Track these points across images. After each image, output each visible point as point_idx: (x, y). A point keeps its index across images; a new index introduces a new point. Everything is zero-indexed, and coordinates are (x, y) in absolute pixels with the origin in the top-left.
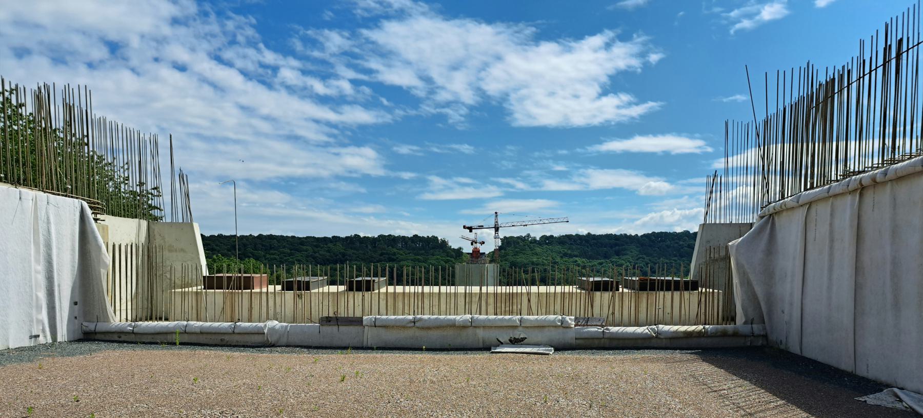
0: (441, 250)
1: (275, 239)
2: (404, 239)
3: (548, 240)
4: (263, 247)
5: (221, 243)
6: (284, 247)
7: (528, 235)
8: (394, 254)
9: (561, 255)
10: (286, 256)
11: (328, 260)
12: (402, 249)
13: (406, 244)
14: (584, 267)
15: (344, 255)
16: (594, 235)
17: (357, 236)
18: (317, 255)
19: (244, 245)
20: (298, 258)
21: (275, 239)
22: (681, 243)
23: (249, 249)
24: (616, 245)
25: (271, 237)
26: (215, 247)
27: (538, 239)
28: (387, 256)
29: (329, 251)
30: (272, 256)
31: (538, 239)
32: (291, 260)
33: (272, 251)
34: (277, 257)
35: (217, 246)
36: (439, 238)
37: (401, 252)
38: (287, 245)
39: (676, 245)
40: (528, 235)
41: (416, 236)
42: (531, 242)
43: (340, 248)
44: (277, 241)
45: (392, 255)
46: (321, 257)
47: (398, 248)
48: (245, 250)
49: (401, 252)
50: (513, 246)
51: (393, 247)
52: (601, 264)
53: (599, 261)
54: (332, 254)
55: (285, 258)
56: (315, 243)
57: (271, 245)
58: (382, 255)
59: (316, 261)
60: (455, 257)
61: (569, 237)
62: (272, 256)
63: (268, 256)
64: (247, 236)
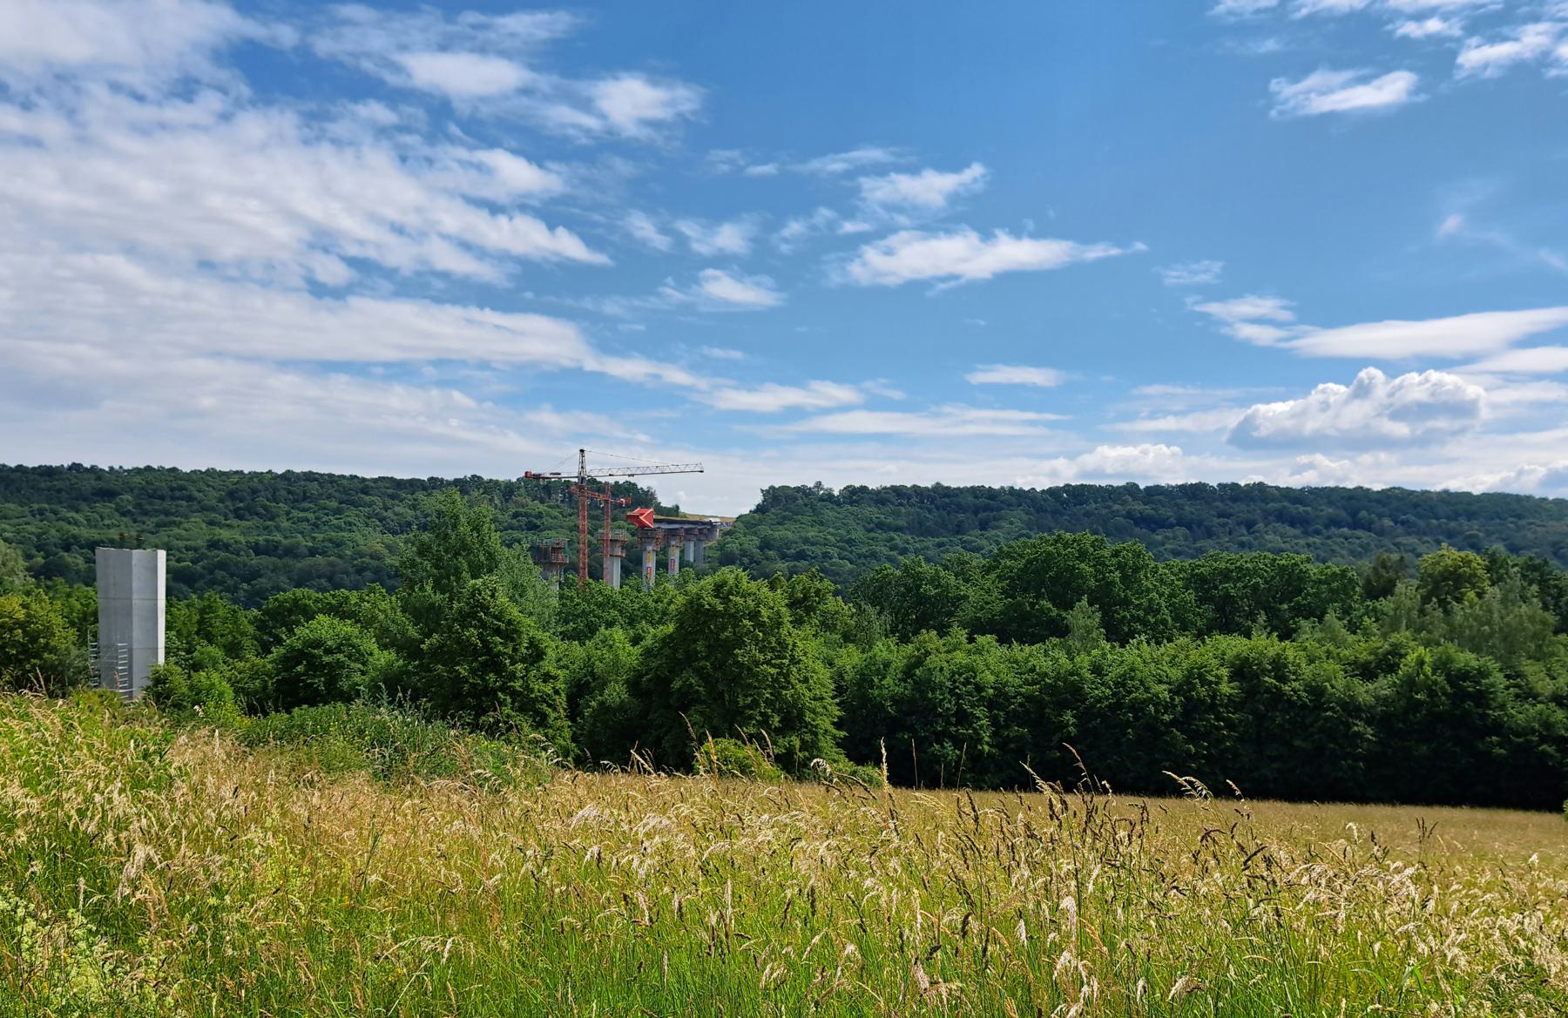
1: (316, 480)
3: (855, 495)
4: (290, 497)
5: (209, 486)
6: (329, 497)
8: (540, 515)
10: (327, 515)
12: (558, 507)
16: (948, 488)
17: (476, 480)
18: (389, 514)
19: (252, 490)
20: (349, 519)
21: (316, 480)
22: (1116, 507)
23: (262, 500)
24: (987, 508)
25: (310, 477)
26: (196, 494)
27: (836, 493)
29: (414, 507)
30: (302, 515)
31: (836, 493)
32: (335, 522)
33: (305, 505)
34: (311, 516)
35: (199, 491)
37: (555, 513)
38: (336, 494)
39: (1104, 511)
40: (819, 485)
42: (821, 499)
44: (320, 484)
46: (395, 518)
48: (253, 500)
49: (555, 513)
51: (542, 502)
53: (936, 540)
54: (418, 512)
55: (325, 519)
56: (390, 491)
57: (304, 492)
58: (516, 515)
59: (384, 525)
61: (898, 491)
62: (302, 515)
63: (295, 513)
64: (262, 473)
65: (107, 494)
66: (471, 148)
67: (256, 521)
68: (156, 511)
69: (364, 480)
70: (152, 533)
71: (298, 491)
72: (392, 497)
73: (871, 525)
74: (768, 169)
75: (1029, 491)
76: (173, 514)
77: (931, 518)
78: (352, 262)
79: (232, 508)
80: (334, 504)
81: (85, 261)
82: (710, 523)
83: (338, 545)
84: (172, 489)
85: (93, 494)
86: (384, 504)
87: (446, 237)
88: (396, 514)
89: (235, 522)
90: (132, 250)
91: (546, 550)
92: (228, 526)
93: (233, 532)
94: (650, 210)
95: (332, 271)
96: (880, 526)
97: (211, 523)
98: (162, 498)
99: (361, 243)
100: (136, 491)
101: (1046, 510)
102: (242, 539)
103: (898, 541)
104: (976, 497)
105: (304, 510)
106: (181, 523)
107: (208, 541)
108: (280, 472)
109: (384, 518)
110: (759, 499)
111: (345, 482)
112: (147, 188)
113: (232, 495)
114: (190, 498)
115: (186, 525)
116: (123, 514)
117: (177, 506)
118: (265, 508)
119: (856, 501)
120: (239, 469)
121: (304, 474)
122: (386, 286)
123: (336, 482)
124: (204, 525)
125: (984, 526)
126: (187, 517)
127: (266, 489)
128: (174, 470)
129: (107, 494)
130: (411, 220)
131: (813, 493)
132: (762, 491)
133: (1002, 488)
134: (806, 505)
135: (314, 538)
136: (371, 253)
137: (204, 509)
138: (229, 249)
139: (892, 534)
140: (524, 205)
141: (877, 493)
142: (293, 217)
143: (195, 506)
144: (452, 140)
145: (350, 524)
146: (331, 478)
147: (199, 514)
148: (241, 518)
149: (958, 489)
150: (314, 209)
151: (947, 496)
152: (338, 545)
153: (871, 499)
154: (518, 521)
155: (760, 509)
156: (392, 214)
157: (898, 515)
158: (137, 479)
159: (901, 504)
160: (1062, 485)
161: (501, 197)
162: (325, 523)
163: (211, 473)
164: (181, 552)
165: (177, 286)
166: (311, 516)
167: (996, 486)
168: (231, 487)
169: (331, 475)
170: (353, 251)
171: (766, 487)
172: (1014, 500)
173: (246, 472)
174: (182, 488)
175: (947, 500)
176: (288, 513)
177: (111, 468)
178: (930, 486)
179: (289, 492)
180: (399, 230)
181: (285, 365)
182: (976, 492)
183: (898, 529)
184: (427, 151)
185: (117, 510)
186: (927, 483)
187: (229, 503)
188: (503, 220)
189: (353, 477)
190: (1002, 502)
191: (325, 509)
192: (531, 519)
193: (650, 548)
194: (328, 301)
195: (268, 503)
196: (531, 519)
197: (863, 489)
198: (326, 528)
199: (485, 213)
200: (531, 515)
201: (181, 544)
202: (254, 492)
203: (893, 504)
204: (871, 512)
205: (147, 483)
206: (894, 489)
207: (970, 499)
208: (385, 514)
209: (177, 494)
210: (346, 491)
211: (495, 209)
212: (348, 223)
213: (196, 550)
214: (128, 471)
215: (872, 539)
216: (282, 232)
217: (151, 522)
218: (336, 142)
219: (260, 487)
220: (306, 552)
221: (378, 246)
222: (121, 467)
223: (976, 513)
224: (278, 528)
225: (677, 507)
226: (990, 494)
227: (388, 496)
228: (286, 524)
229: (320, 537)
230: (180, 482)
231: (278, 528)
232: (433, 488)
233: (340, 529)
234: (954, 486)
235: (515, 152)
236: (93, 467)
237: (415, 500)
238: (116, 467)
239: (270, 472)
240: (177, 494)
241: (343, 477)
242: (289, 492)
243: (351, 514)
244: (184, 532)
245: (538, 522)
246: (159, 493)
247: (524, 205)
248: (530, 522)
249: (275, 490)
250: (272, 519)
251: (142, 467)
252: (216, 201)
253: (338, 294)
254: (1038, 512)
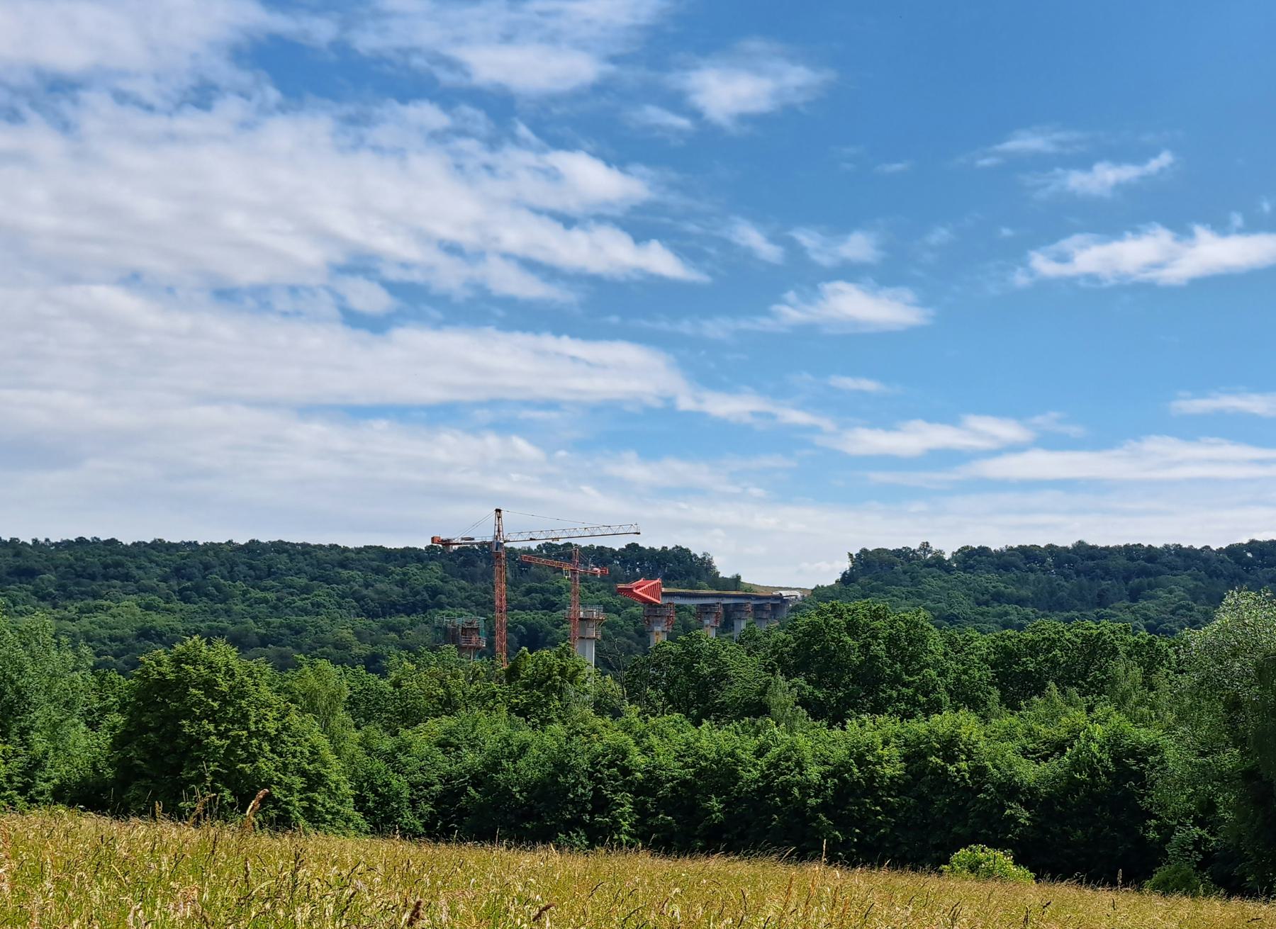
2: (601, 554)
3: (972, 558)
5: (151, 561)
6: (299, 572)
7: (925, 547)
10: (292, 594)
11: (393, 605)
15: (434, 592)
18: (368, 592)
20: (318, 599)
21: (286, 551)
23: (215, 577)
25: (280, 547)
26: (134, 572)
27: (947, 556)
29: (401, 584)
30: (261, 595)
31: (947, 556)
32: (299, 603)
33: (269, 582)
34: (271, 596)
35: (138, 568)
42: (927, 565)
43: (434, 573)
44: (290, 555)
45: (554, 594)
46: (376, 597)
48: (204, 578)
54: (407, 590)
56: (375, 564)
57: (270, 567)
58: (529, 592)
59: (362, 606)
61: (1028, 554)
62: (261, 595)
64: (220, 544)
65: (27, 574)
66: (541, 151)
67: (204, 603)
68: (82, 593)
69: (346, 549)
70: (73, 620)
71: (262, 566)
72: (377, 571)
73: (986, 597)
74: (897, 167)
75: (1201, 550)
76: (102, 597)
78: (393, 288)
79: (176, 588)
80: (303, 581)
81: (77, 295)
82: (780, 597)
83: (298, 633)
84: (106, 567)
85: (9, 574)
86: (365, 580)
87: (507, 256)
88: (378, 592)
89: (177, 605)
90: (132, 280)
91: (455, 630)
92: (167, 610)
93: (171, 617)
94: (758, 219)
95: (367, 297)
96: (998, 597)
97: (148, 607)
98: (93, 577)
99: (405, 265)
100: (62, 569)
101: (1222, 574)
102: (179, 626)
103: (1014, 618)
104: (1131, 559)
105: (264, 589)
106: (109, 608)
107: (138, 629)
108: (242, 543)
109: (363, 598)
110: (846, 565)
111: (320, 554)
112: (151, 208)
113: (179, 572)
114: (127, 577)
115: (114, 611)
116: (43, 598)
117: (109, 587)
118: (217, 587)
119: (972, 567)
120: (193, 540)
121: (273, 544)
122: (437, 314)
123: (308, 553)
124: (138, 610)
125: (1135, 596)
126: (119, 601)
127: (223, 564)
128: (113, 542)
129: (27, 574)
130: (467, 237)
131: (919, 557)
132: (851, 556)
133: (1166, 547)
134: (905, 572)
135: (268, 624)
136: (416, 276)
137: (143, 590)
138: (248, 273)
139: (1008, 608)
140: (599, 216)
141: (1000, 554)
142: (323, 236)
143: (131, 586)
144: (516, 141)
145: (319, 605)
146: (306, 550)
147: (135, 597)
148: (186, 600)
149: (1107, 548)
150: (350, 228)
151: (1092, 558)
152: (298, 633)
153: (992, 564)
154: (531, 599)
155: (846, 579)
156: (445, 231)
157: (1022, 582)
158: (65, 554)
159: (1032, 570)
160: (1245, 541)
161: (571, 204)
162: (287, 605)
163: (158, 545)
164: (105, 644)
165: (184, 322)
166: (271, 596)
167: (1158, 544)
168: (179, 561)
169: (305, 545)
170: (393, 274)
171: (855, 551)
172: (1179, 562)
173: (201, 543)
174: (118, 565)
175: (1091, 563)
176: (245, 593)
177: (35, 541)
178: (1070, 546)
179: (251, 567)
180: (452, 249)
181: (308, 410)
182: (1130, 552)
183: (1021, 602)
184: (486, 157)
185: (35, 593)
187: (173, 583)
188: (577, 235)
189: (334, 547)
190: (1164, 564)
191: (290, 587)
192: (547, 595)
193: (658, 629)
194: (364, 335)
195: (222, 581)
196: (547, 595)
197: (983, 551)
198: (287, 611)
199: (559, 227)
200: (548, 591)
201: (104, 633)
202: (207, 567)
203: (1017, 568)
204: (990, 580)
205: (76, 559)
206: (1023, 550)
207: (1122, 561)
208: (365, 592)
209: (112, 571)
210: (319, 564)
211: (568, 221)
212: (391, 244)
213: (122, 640)
214: (56, 544)
215: (982, 614)
216: (310, 255)
217: (73, 607)
218: (377, 149)
219: (215, 561)
220: (255, 639)
221: (430, 268)
222: (47, 540)
223: (1127, 579)
224: (228, 612)
225: (738, 578)
226: (1151, 554)
227: (373, 569)
228: (239, 607)
229: (276, 621)
230: (117, 558)
231: (228, 612)
232: (431, 559)
233: (307, 613)
234: (1102, 544)
235: (596, 155)
236: (13, 540)
237: (405, 574)
238: (42, 540)
239: (230, 542)
240: (112, 571)
241: (321, 547)
242: (251, 567)
243: (321, 593)
244: (110, 620)
245: (556, 599)
246: (89, 571)
247: (599, 216)
248: (546, 600)
249: (233, 565)
250: (223, 601)
251: (73, 538)
252: (236, 221)
253: (376, 325)
254: (1210, 577)
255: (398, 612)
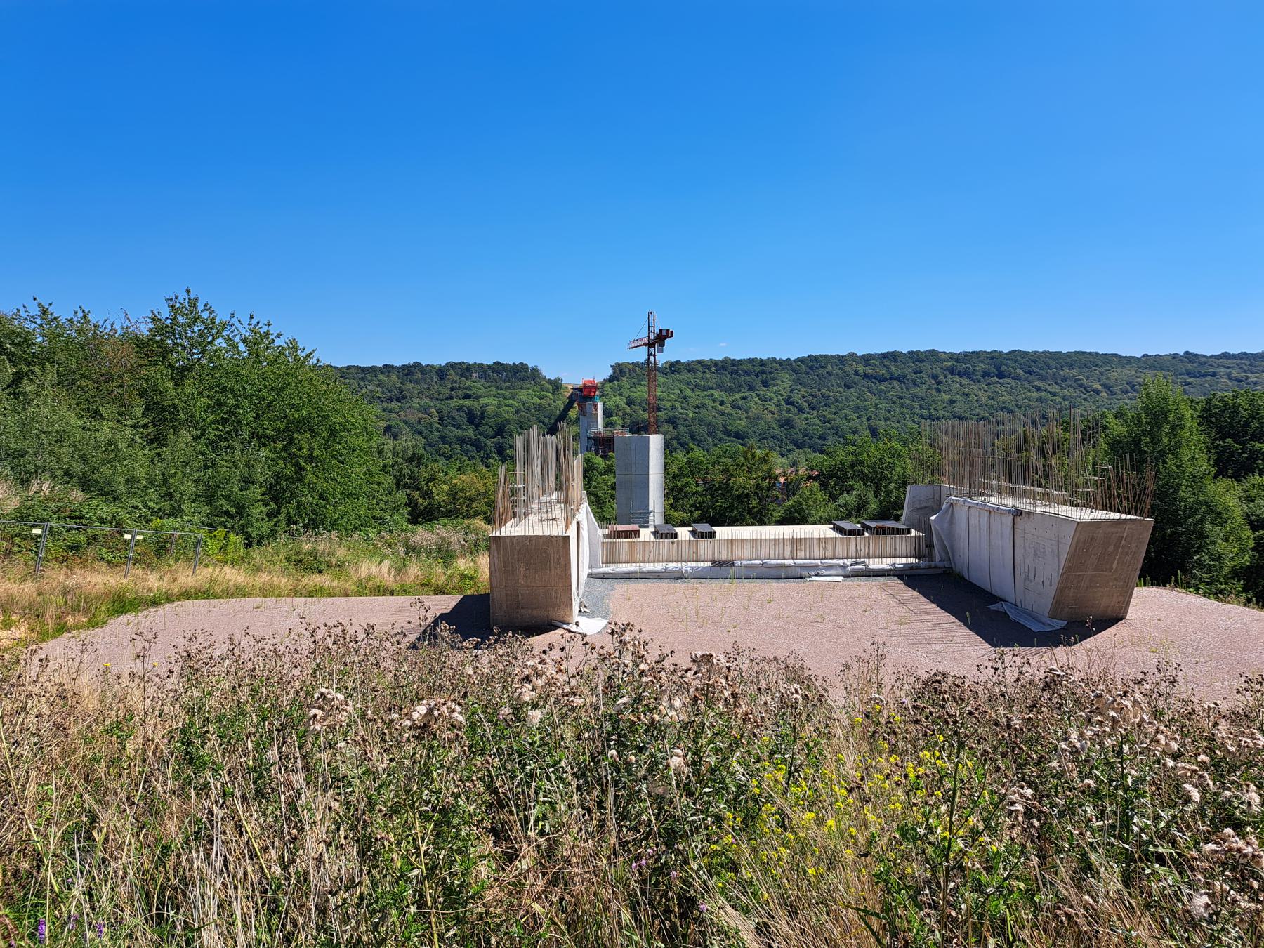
0: (533, 382)
8: (469, 388)
9: (692, 386)
13: (485, 373)
14: (722, 403)
28: (460, 391)
36: (530, 366)
41: (498, 363)
47: (474, 380)
49: (479, 386)
50: (628, 376)
52: (744, 398)
58: (452, 389)
60: (551, 391)
77: (727, 380)
110: (610, 372)
119: (674, 371)
133: (769, 359)
149: (740, 360)
175: (735, 368)
182: (751, 361)
186: (719, 357)
197: (678, 362)
206: (699, 362)
226: (762, 363)
234: (738, 358)
255: (382, 401)
